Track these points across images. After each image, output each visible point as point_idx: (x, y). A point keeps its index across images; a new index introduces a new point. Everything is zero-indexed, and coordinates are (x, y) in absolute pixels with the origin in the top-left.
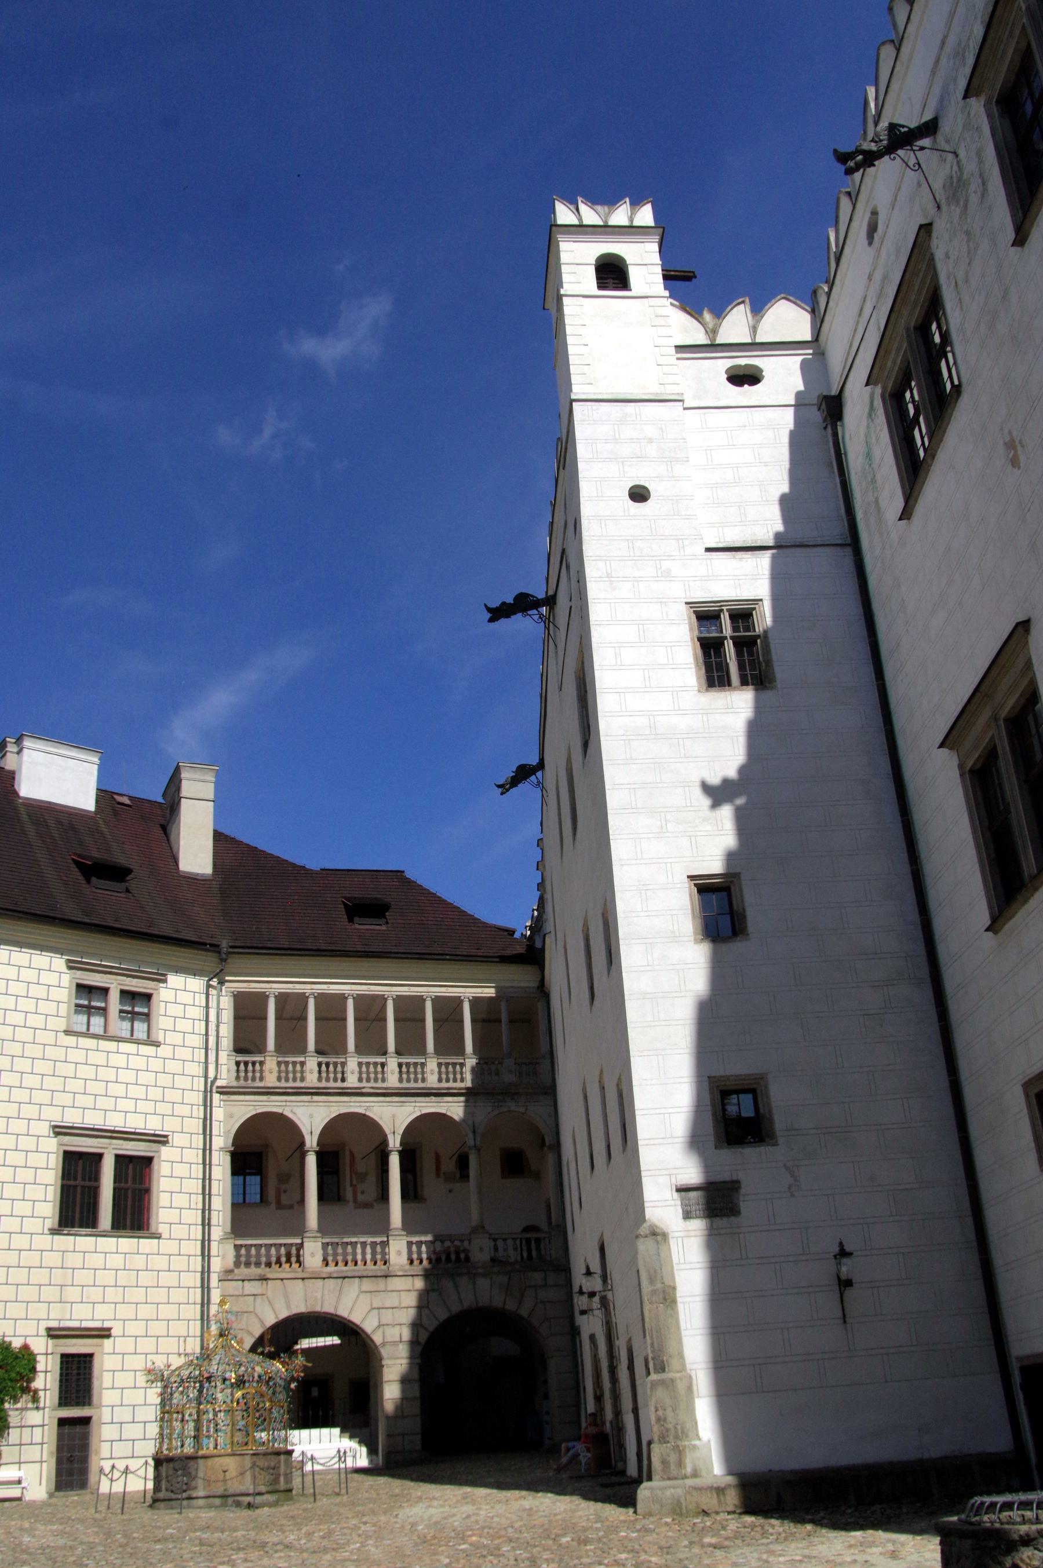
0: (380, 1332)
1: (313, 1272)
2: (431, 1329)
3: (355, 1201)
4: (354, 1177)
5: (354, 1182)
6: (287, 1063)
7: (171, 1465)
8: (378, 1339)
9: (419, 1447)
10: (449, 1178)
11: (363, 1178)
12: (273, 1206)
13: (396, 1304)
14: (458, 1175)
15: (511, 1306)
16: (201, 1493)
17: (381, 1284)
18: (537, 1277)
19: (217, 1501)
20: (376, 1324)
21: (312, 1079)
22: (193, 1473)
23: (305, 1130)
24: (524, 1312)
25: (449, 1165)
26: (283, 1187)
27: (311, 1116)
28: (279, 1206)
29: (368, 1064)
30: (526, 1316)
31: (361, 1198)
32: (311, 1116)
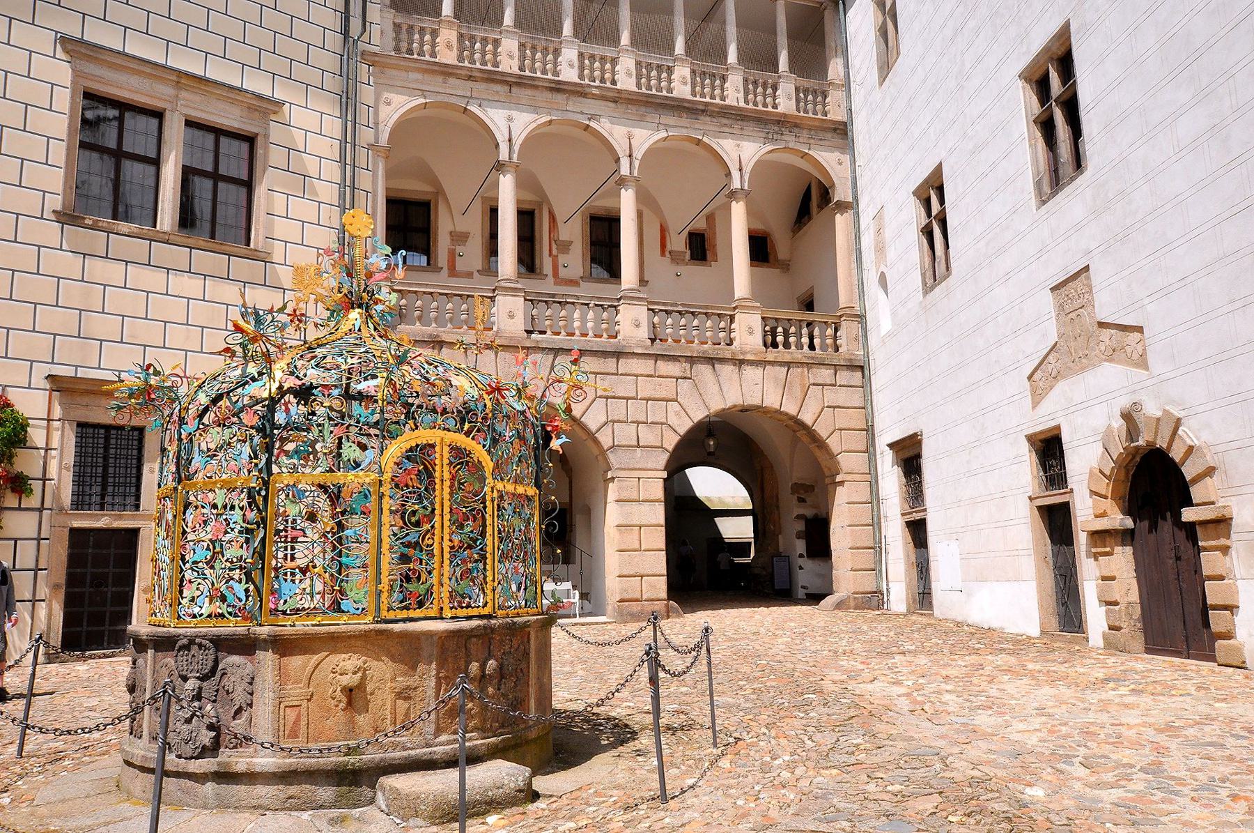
0: (607, 430)
1: (511, 338)
2: (682, 431)
3: (555, 274)
4: (554, 247)
5: (555, 252)
6: (473, 39)
7: (169, 660)
8: (605, 439)
9: (664, 595)
10: (676, 258)
11: (565, 247)
12: (445, 272)
13: (633, 394)
14: (688, 256)
15: (790, 408)
16: (266, 761)
17: (610, 364)
18: (825, 374)
19: (326, 793)
20: (604, 419)
21: (509, 64)
22: (239, 697)
23: (501, 137)
24: (807, 417)
25: (678, 243)
26: (459, 249)
27: (510, 119)
28: (453, 272)
29: (592, 57)
30: (809, 421)
31: (562, 273)
32: (510, 119)
